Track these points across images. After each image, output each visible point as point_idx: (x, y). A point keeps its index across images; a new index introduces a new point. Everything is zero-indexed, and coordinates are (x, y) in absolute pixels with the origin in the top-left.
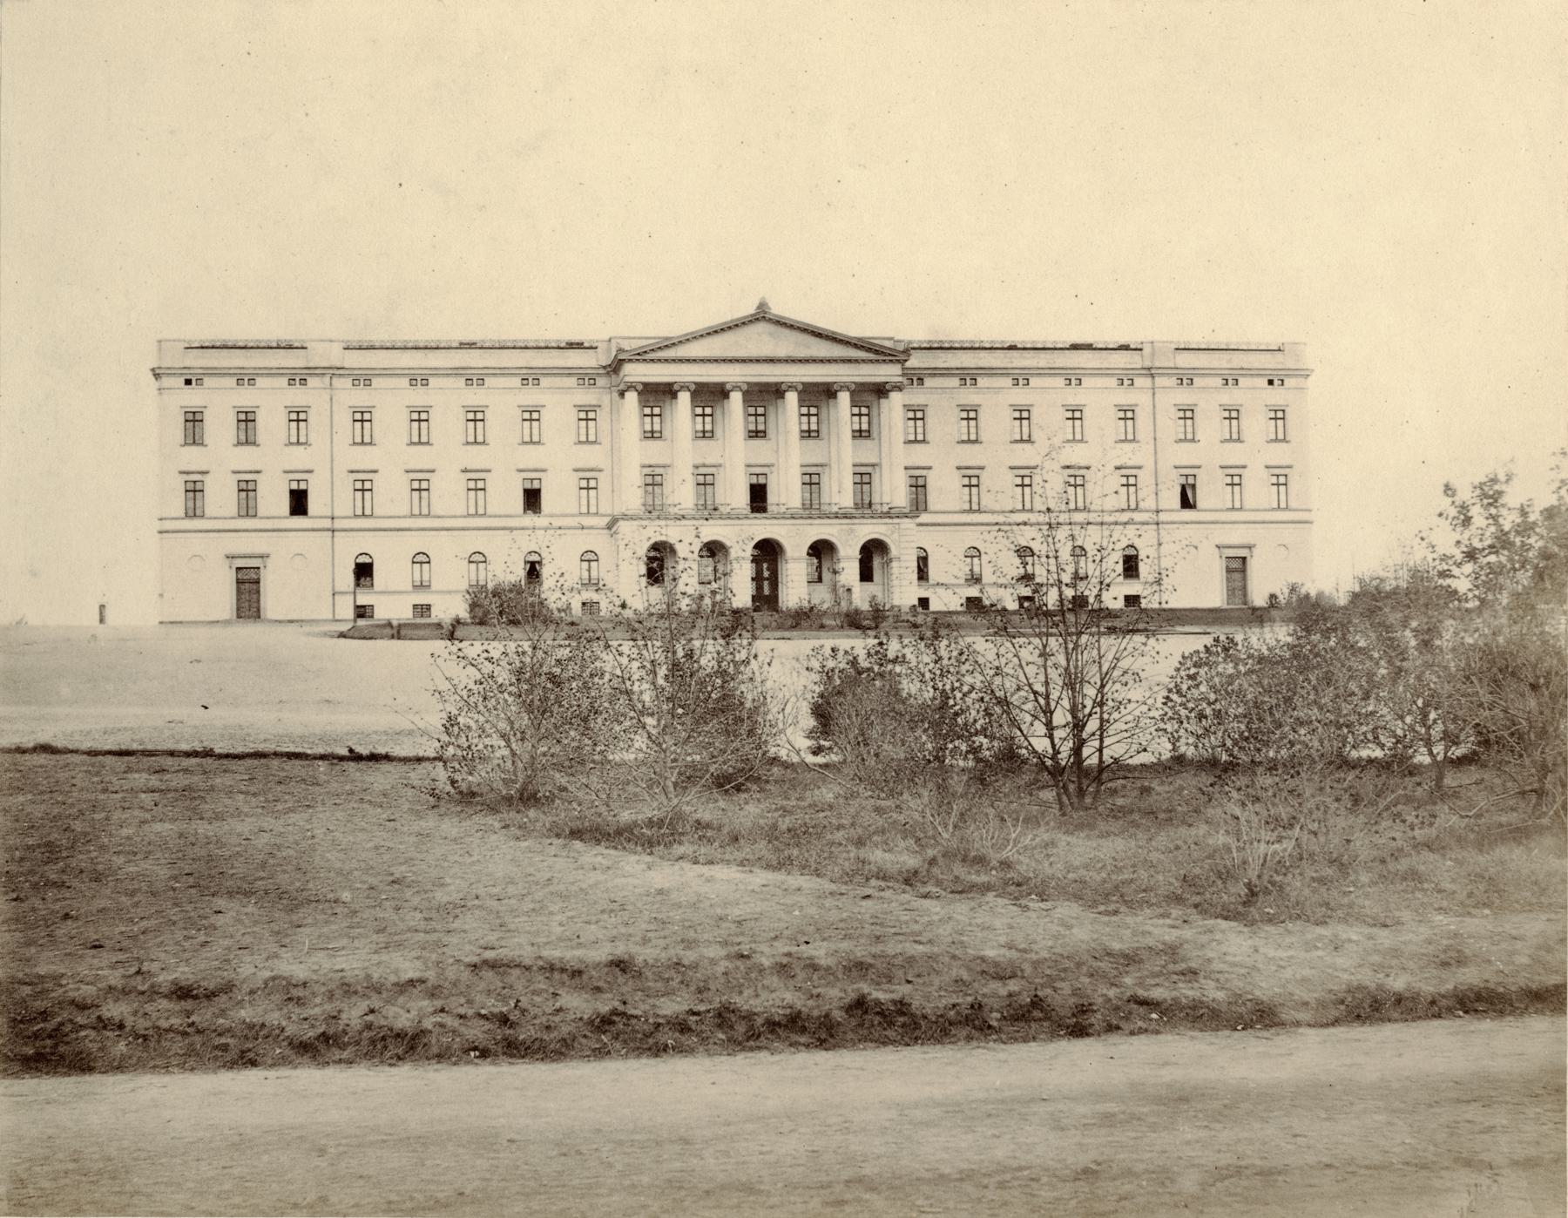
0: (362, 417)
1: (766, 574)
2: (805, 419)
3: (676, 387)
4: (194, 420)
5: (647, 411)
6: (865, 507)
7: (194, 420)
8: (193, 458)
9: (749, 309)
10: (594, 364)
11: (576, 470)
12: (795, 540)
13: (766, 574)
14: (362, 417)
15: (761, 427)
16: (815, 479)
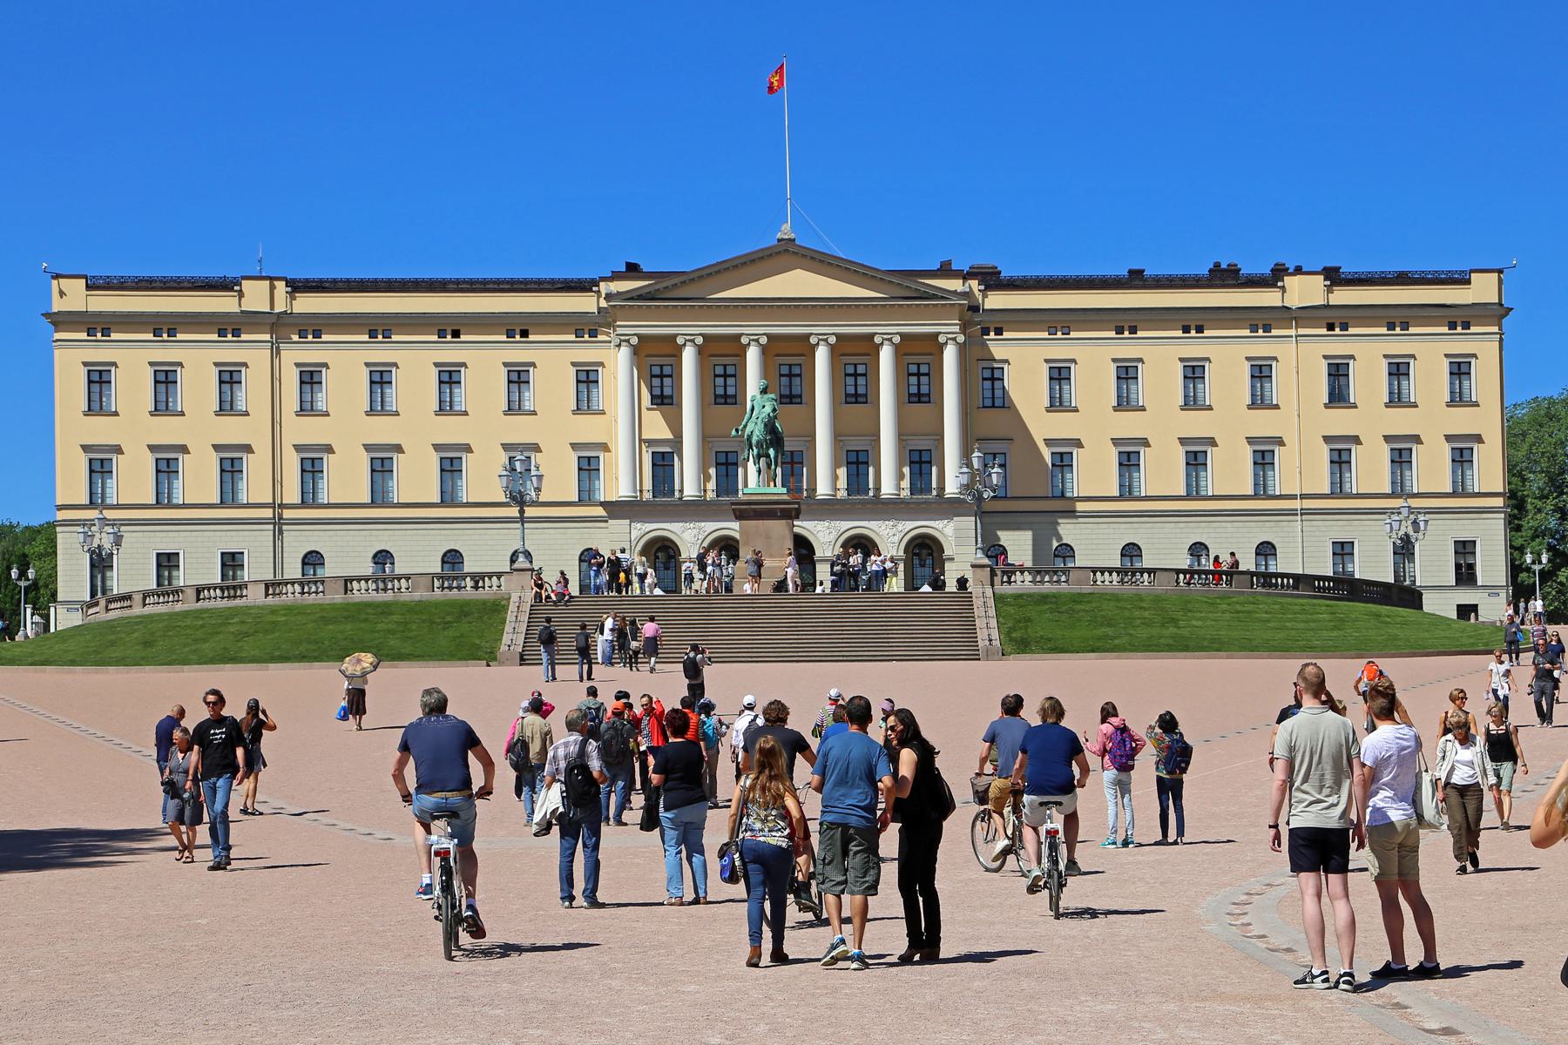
0: (310, 378)
14: (310, 378)
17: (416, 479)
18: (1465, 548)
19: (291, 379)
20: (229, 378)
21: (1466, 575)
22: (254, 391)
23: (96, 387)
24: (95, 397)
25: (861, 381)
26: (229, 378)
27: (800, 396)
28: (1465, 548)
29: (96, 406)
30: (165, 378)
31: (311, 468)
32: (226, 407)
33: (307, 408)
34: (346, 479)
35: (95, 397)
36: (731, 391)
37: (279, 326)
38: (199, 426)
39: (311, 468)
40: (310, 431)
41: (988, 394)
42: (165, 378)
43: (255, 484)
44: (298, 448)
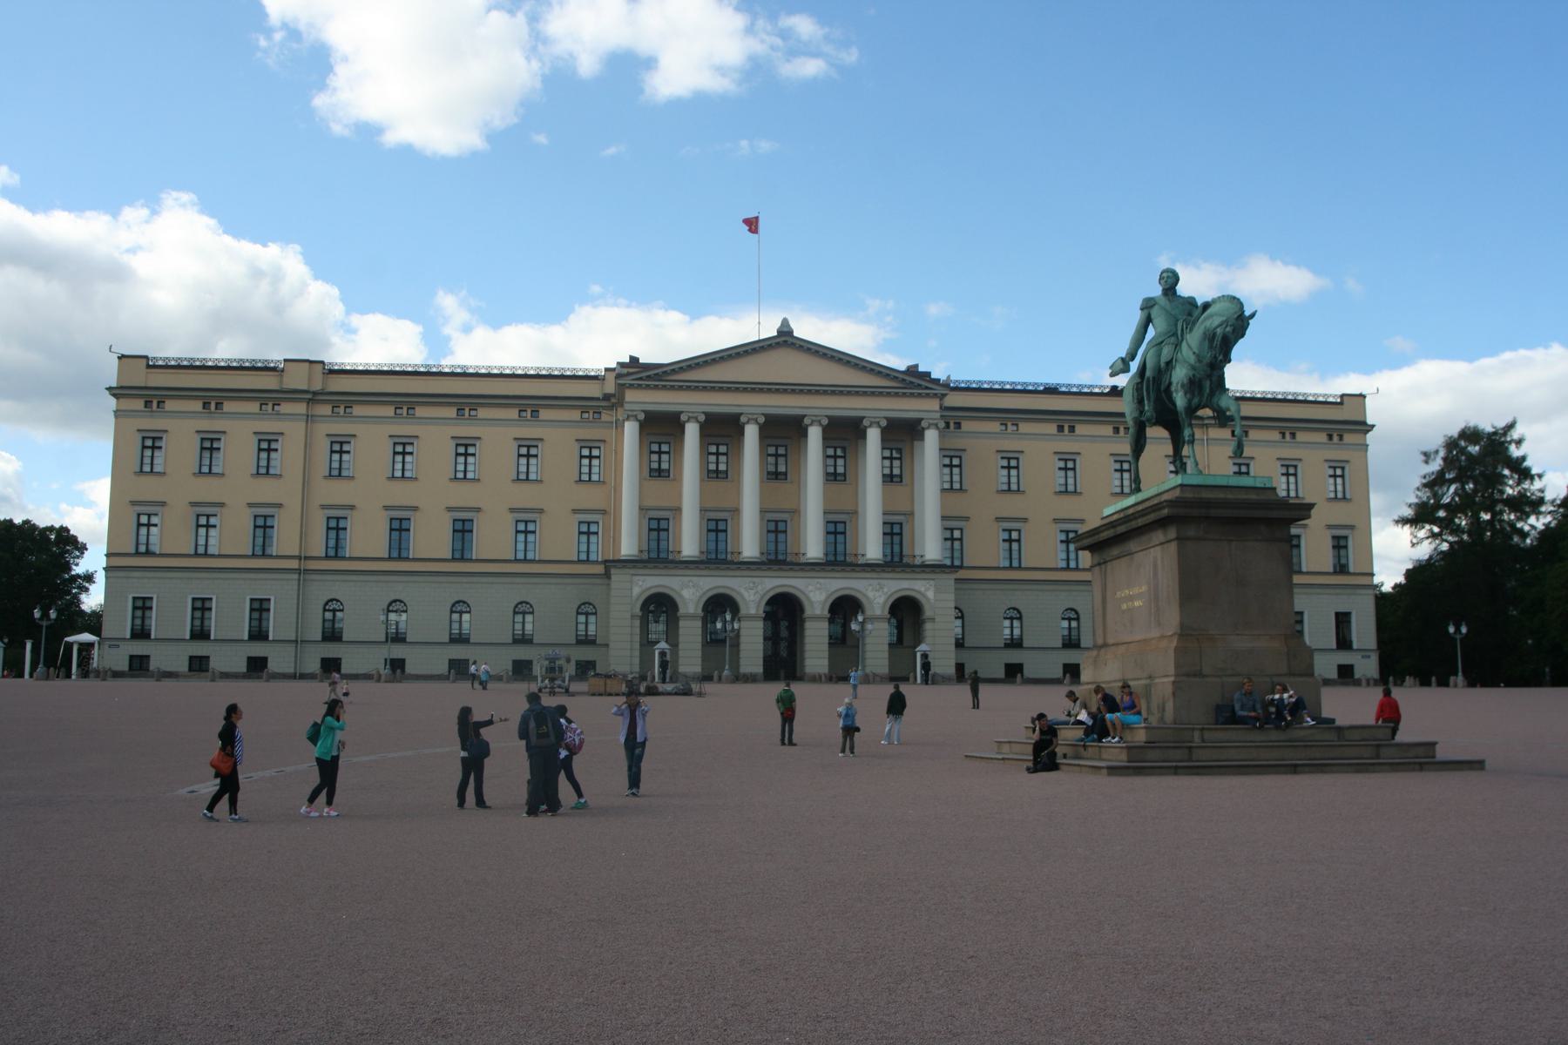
0: (339, 446)
1: (784, 633)
2: (831, 462)
3: (683, 418)
4: (152, 442)
5: (655, 447)
6: (897, 560)
7: (152, 442)
8: (149, 488)
9: (769, 331)
10: (598, 394)
11: (575, 511)
12: (817, 594)
13: (784, 633)
15: (782, 469)
16: (840, 528)
17: (430, 538)
18: (1343, 620)
19: (323, 446)
20: (267, 444)
21: (1344, 643)
22: (288, 456)
23: (148, 453)
24: (147, 460)
25: (840, 462)
26: (267, 444)
27: (785, 474)
28: (1343, 620)
29: (147, 468)
30: (210, 445)
31: (336, 527)
32: (264, 472)
33: (337, 474)
34: (368, 537)
35: (147, 460)
36: (722, 467)
37: (313, 397)
38: (237, 486)
39: (336, 527)
40: (337, 493)
41: (947, 478)
42: (210, 445)
43: (285, 539)
44: (323, 507)
